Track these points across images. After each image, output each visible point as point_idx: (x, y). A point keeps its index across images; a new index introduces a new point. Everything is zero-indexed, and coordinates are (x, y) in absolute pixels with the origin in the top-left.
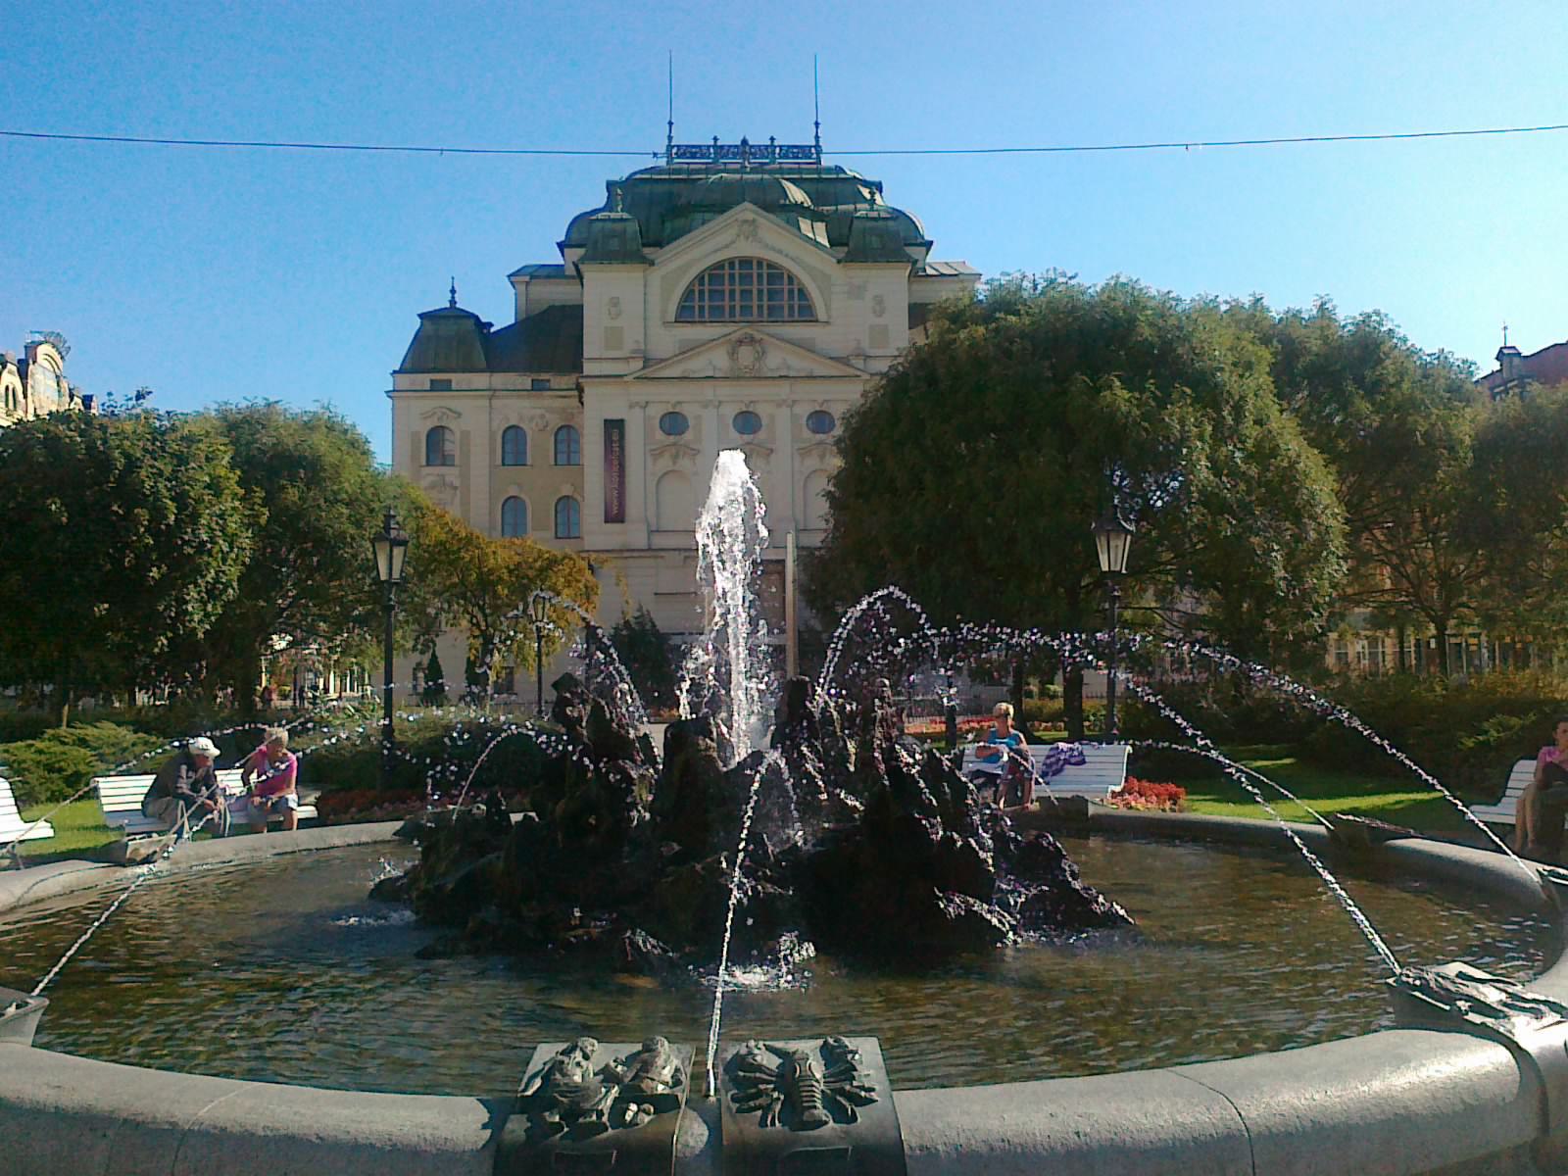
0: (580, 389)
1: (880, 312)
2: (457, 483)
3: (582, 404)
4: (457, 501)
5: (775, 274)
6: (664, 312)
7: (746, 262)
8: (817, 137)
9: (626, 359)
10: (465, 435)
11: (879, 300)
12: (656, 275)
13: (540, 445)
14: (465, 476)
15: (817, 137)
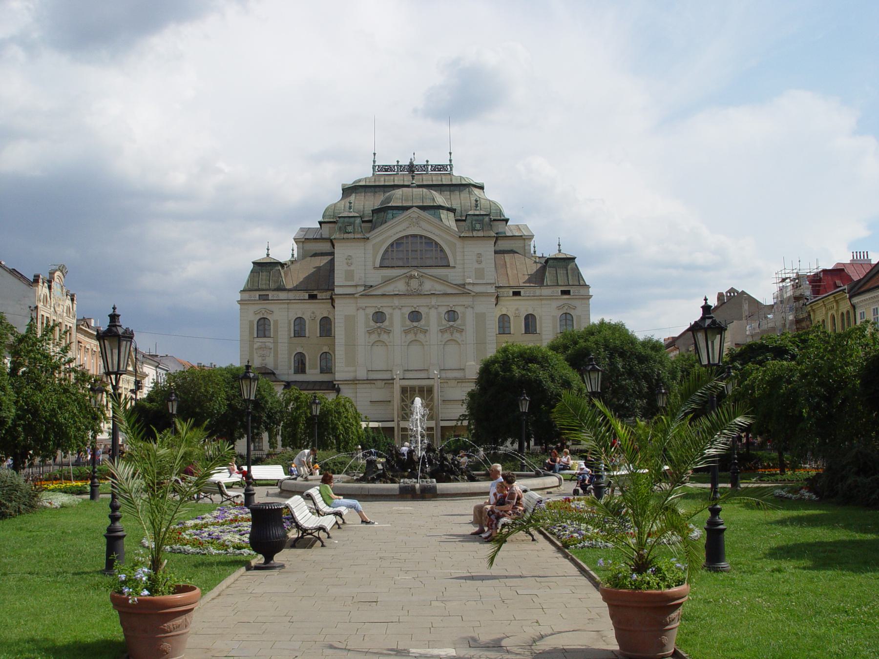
0: (332, 299)
1: (479, 262)
2: (272, 346)
3: (334, 307)
4: (272, 355)
5: (430, 242)
6: (374, 263)
7: (414, 236)
8: (450, 161)
9: (356, 286)
10: (276, 322)
11: (479, 255)
12: (370, 245)
13: (312, 329)
14: (276, 343)
15: (450, 161)
